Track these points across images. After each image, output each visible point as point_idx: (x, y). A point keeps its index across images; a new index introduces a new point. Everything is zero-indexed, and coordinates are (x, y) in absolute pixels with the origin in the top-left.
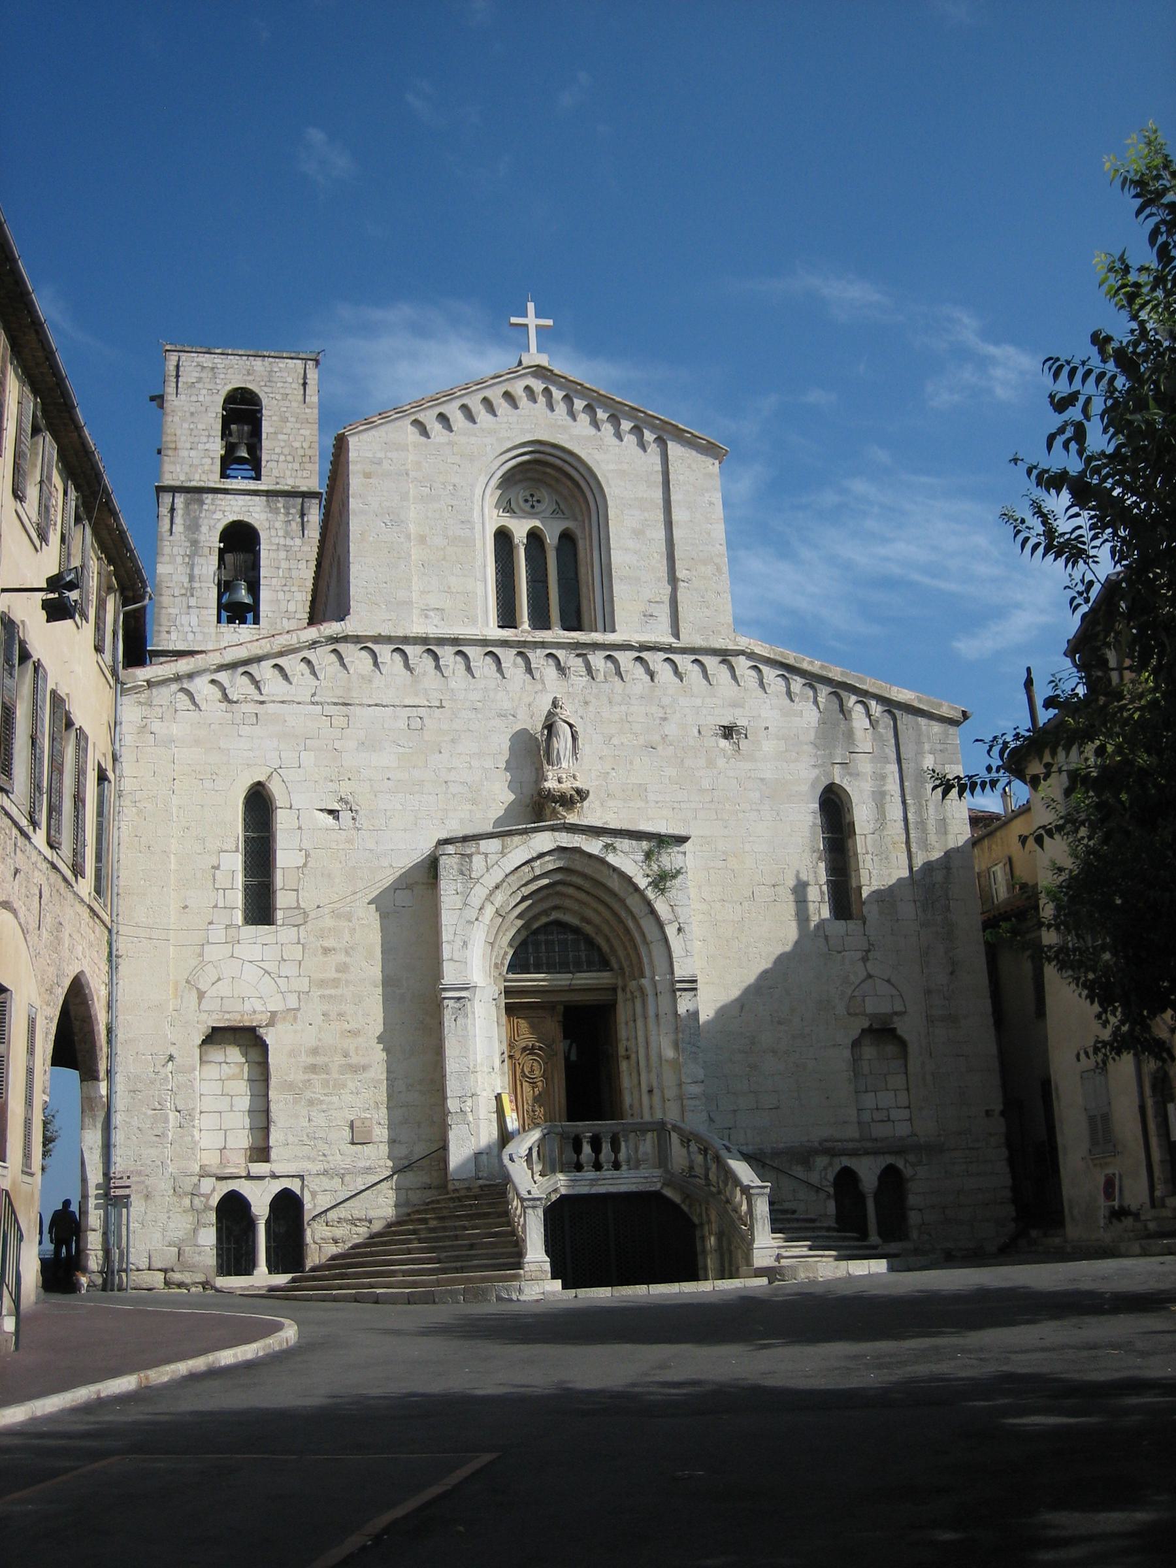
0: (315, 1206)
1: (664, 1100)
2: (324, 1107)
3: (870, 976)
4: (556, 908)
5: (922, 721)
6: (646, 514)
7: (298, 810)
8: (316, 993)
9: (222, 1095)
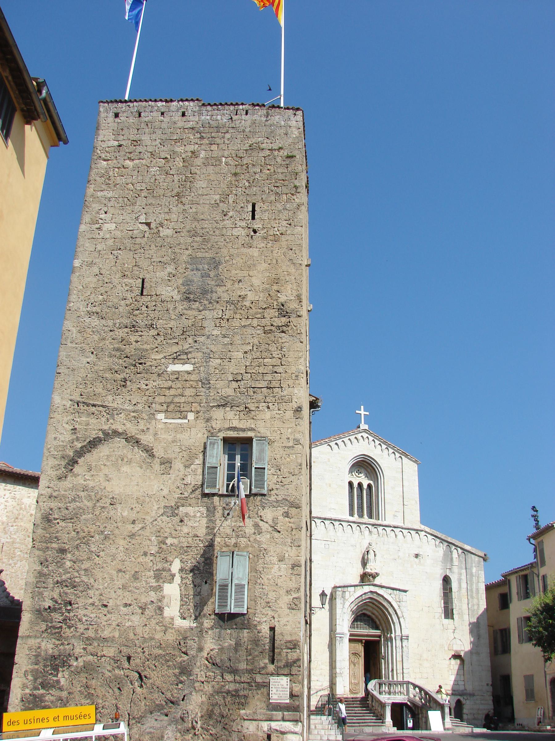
3: (455, 638)
4: (365, 609)
5: (473, 556)
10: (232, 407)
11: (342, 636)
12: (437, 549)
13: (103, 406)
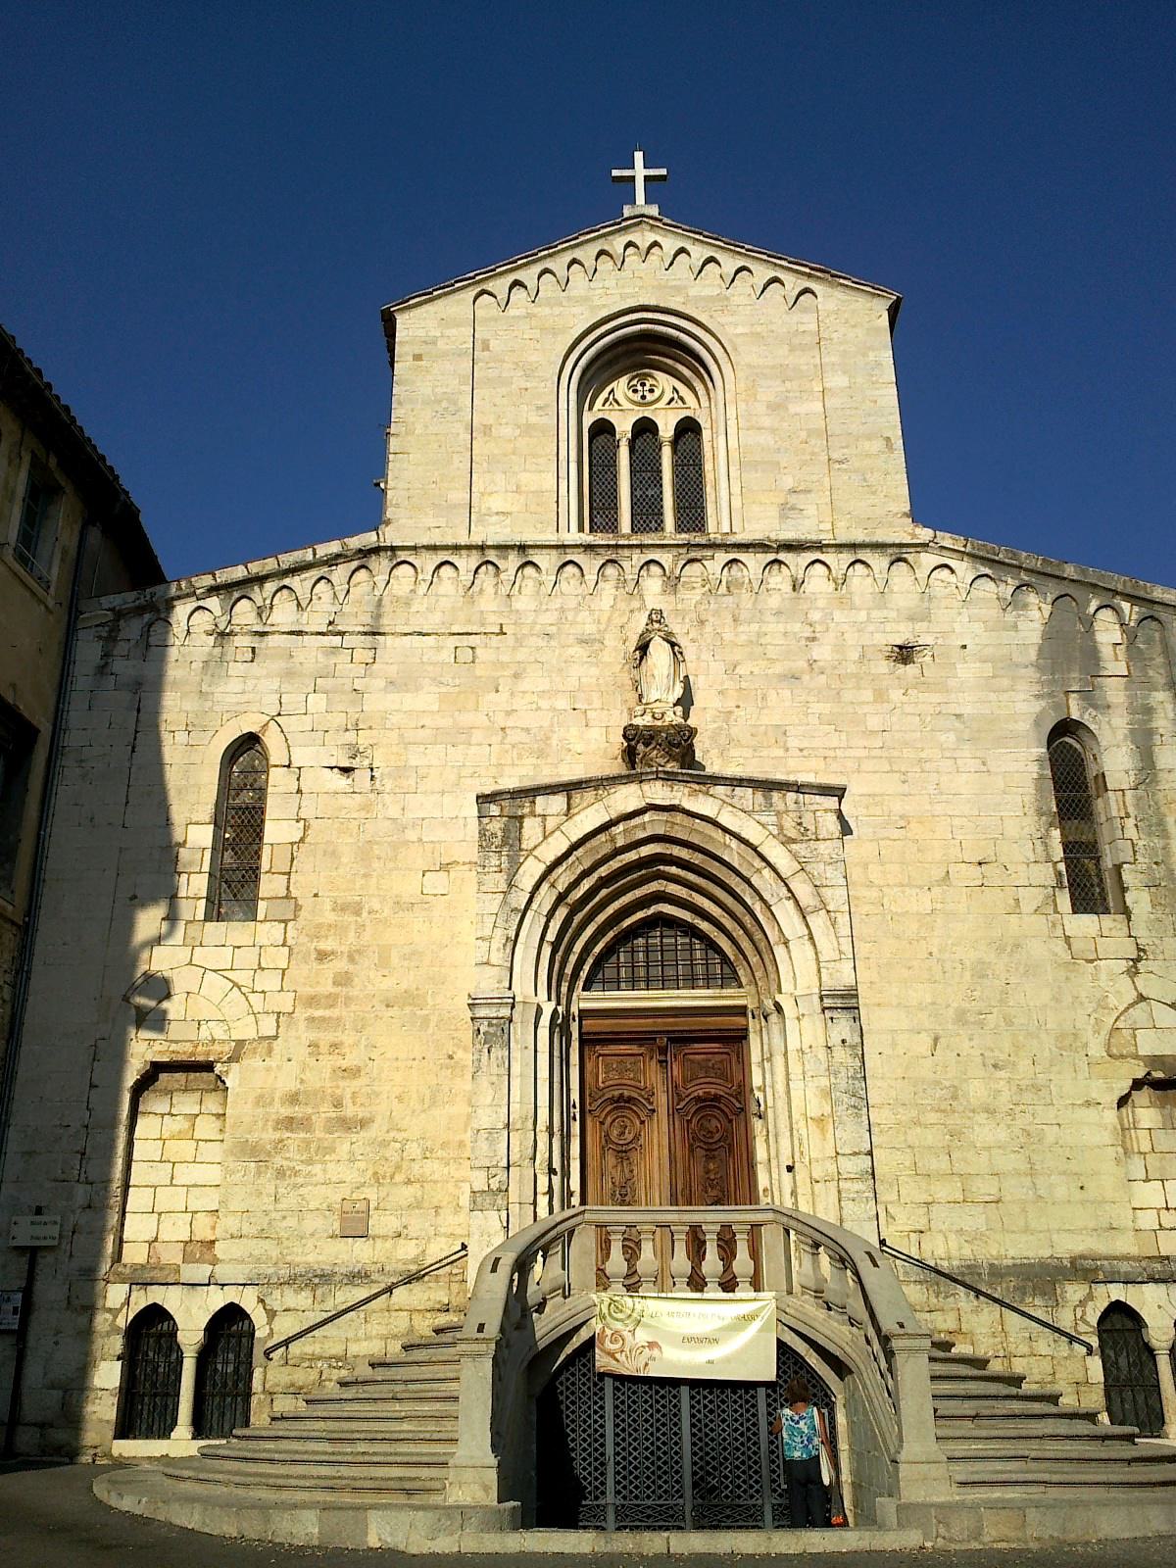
0: (271, 1334)
2: (300, 1180)
3: (1142, 998)
6: (788, 384)
7: (299, 768)
8: (301, 1014)
9: (161, 1162)
11: (505, 1012)
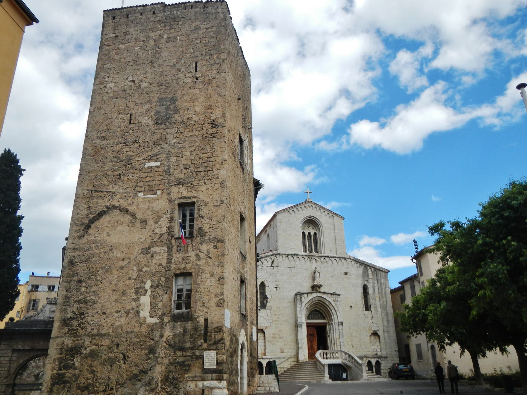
1: (337, 346)
5: (381, 272)
10: (183, 185)
12: (358, 269)
13: (106, 192)
